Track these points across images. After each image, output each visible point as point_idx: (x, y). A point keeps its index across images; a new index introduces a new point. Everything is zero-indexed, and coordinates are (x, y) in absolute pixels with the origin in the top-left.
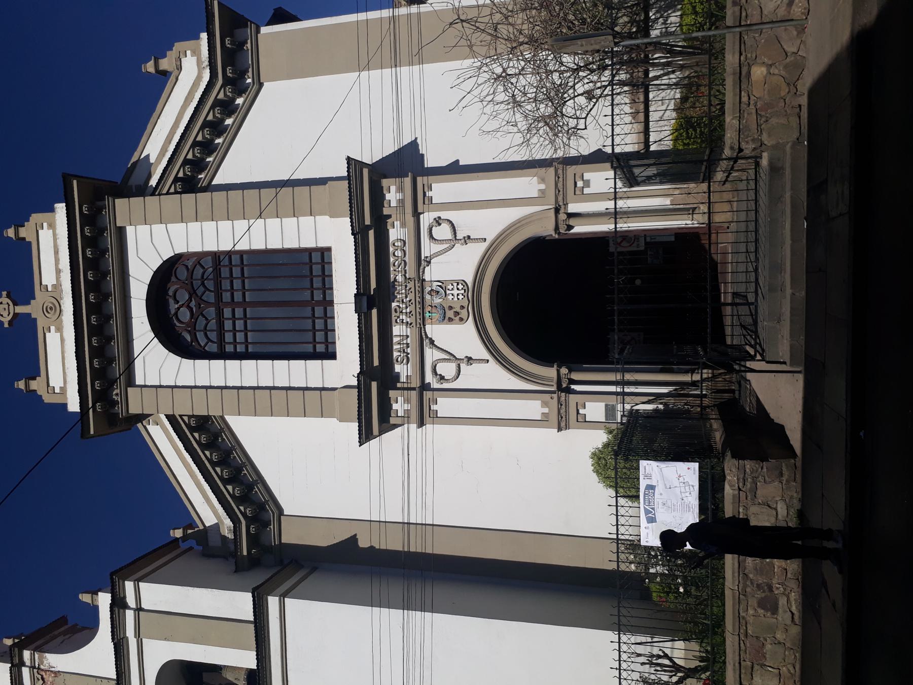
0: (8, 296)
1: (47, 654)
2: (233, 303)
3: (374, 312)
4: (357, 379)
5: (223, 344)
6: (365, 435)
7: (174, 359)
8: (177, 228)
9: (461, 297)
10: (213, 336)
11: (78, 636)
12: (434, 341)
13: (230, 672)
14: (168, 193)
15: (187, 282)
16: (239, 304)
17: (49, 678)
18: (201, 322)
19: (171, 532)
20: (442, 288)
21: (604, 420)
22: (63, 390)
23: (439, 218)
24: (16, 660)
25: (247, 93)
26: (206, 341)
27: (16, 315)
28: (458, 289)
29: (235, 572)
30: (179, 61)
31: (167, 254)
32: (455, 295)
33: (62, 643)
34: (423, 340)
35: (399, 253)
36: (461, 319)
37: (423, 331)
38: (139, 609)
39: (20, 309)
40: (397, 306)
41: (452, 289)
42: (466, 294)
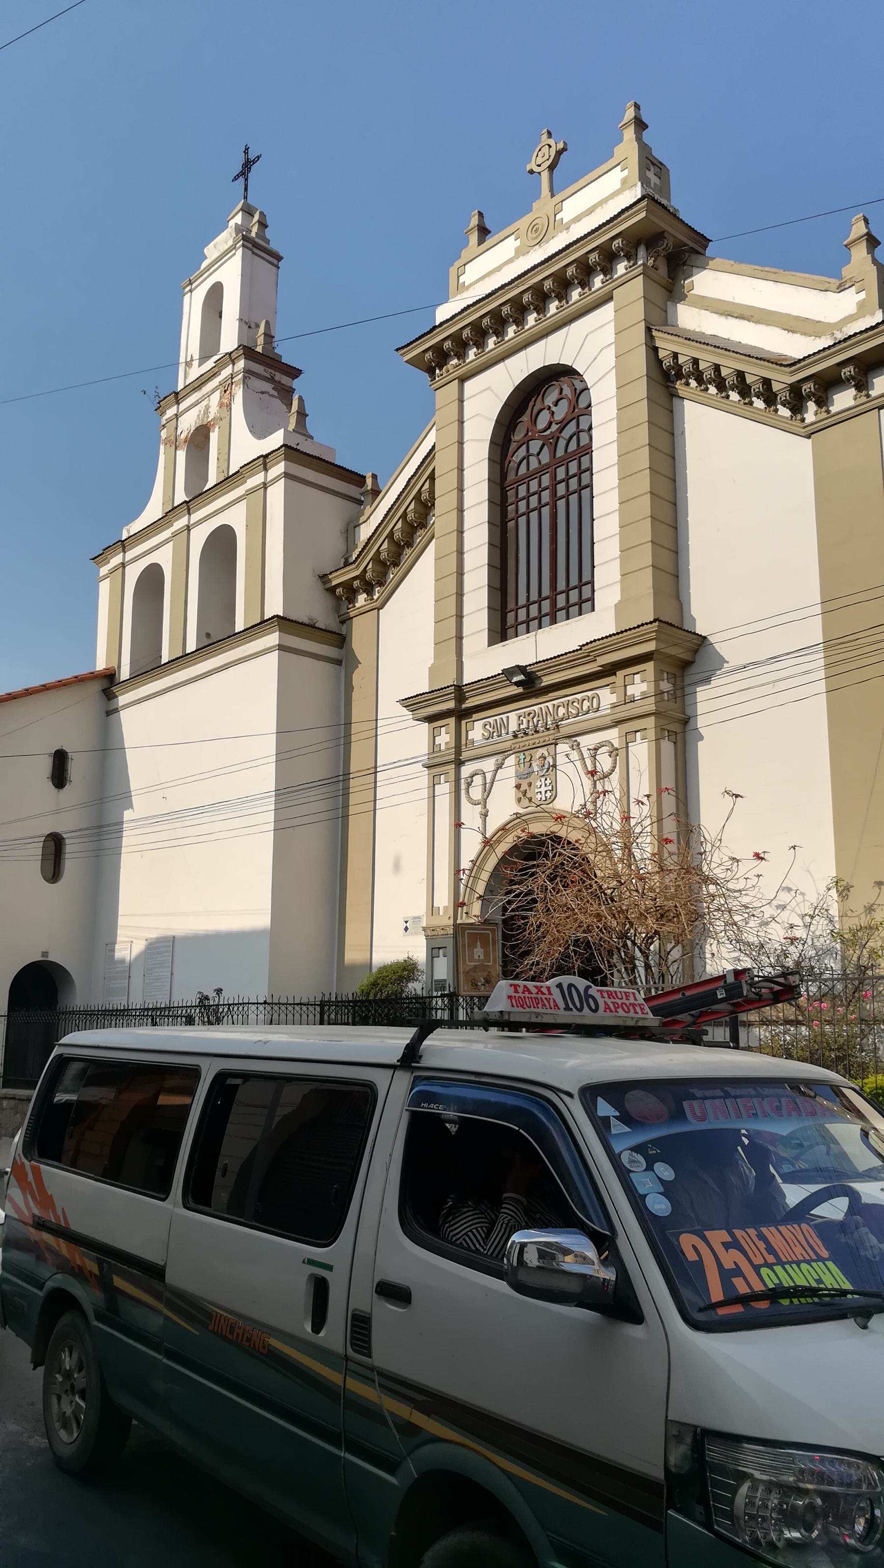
0: (559, 153)
2: (555, 483)
6: (411, 703)
9: (539, 796)
12: (501, 767)
14: (653, 349)
15: (576, 410)
16: (554, 492)
18: (535, 446)
20: (547, 771)
21: (435, 978)
22: (461, 288)
23: (617, 755)
25: (790, 422)
30: (852, 283)
32: (540, 790)
35: (586, 704)
36: (519, 800)
37: (509, 753)
38: (265, 486)
41: (546, 785)
42: (542, 802)
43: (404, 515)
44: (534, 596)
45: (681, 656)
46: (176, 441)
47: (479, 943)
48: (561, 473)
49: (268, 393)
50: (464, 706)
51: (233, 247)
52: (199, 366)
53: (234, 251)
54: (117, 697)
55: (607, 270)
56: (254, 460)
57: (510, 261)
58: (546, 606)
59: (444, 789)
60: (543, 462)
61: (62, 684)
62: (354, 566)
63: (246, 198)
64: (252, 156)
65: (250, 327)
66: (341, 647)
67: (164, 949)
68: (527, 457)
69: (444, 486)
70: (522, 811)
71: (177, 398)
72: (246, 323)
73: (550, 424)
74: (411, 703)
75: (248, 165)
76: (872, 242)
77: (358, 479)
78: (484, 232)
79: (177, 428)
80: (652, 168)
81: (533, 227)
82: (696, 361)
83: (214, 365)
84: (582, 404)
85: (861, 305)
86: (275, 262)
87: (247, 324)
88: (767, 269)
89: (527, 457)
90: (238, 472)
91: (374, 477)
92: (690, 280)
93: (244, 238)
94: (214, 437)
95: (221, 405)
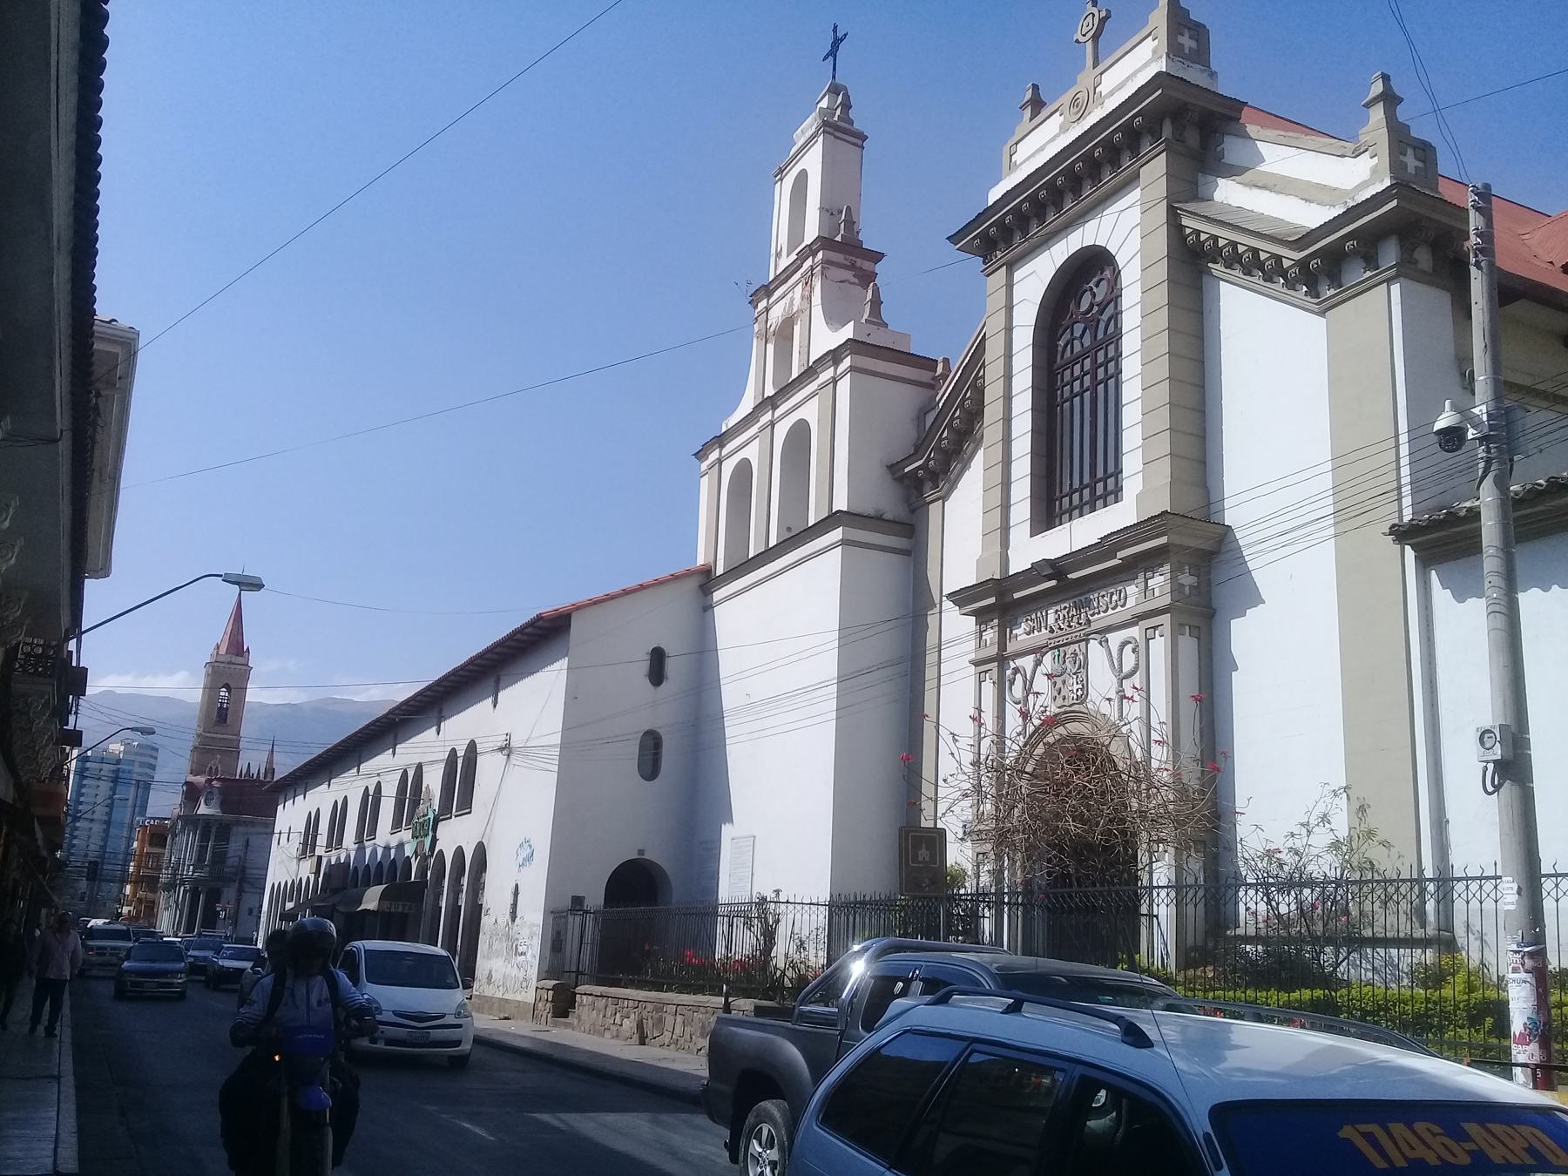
0: (1103, 21)
2: (1096, 366)
3: (1053, 583)
8: (1137, 264)
18: (1078, 328)
22: (1012, 167)
25: (1309, 299)
28: (1077, 690)
29: (887, 466)
31: (1121, 260)
32: (1073, 685)
33: (842, 282)
34: (1039, 651)
35: (1115, 598)
38: (835, 381)
40: (1068, 613)
41: (1077, 683)
42: (1075, 701)
44: (1076, 485)
45: (1202, 547)
47: (924, 846)
48: (1101, 358)
49: (848, 281)
51: (814, 136)
55: (1134, 149)
56: (824, 355)
57: (1053, 139)
58: (1086, 492)
59: (989, 689)
60: (1086, 345)
61: (659, 583)
63: (834, 77)
64: (840, 35)
65: (832, 214)
66: (911, 538)
67: (746, 849)
68: (1070, 342)
69: (993, 372)
70: (1058, 710)
71: (767, 290)
72: (827, 210)
73: (1092, 306)
74: (962, 598)
75: (837, 43)
76: (1390, 99)
77: (929, 364)
78: (1037, 104)
80: (1186, 31)
81: (1074, 102)
82: (1215, 238)
84: (1118, 287)
85: (1374, 171)
86: (859, 142)
87: (827, 211)
88: (1290, 134)
89: (1070, 342)
91: (946, 361)
92: (1222, 146)
93: (825, 124)
94: (797, 329)
95: (803, 297)
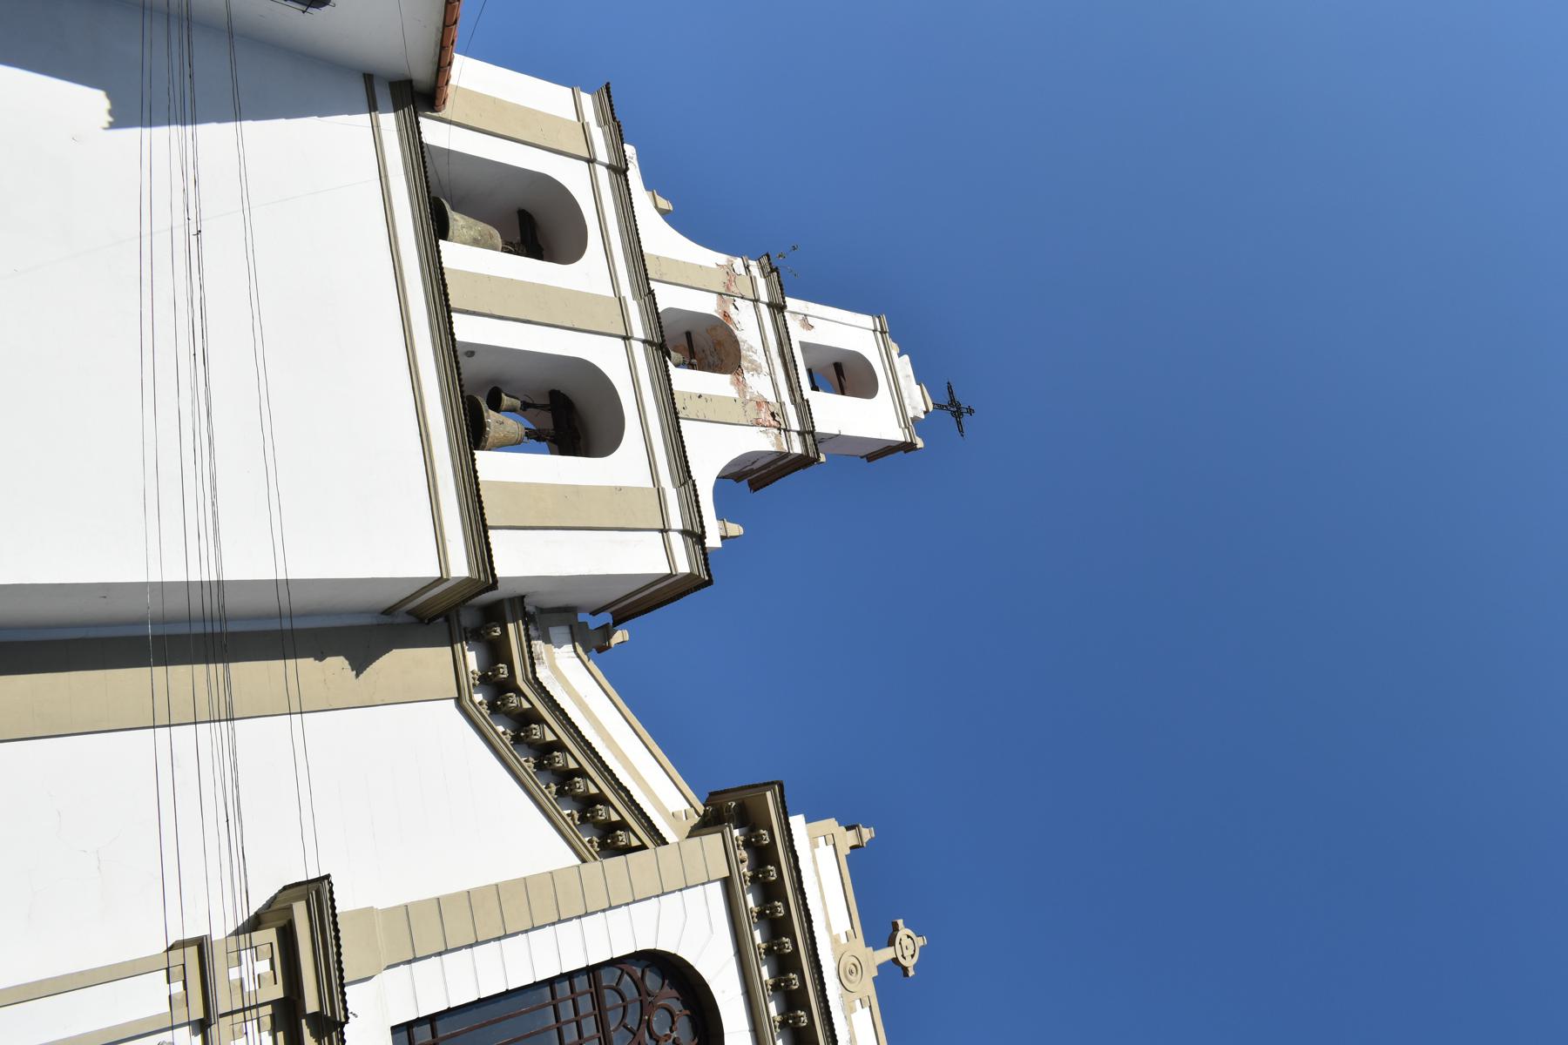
0: (905, 969)
1: (773, 449)
4: (349, 1011)
5: (593, 990)
6: (317, 891)
7: (664, 946)
10: (611, 999)
11: (736, 469)
13: (513, 433)
17: (765, 416)
19: (627, 638)
22: (814, 845)
24: (809, 439)
26: (621, 987)
27: (891, 942)
29: (523, 597)
38: (664, 531)
39: (887, 954)
43: (581, 772)
46: (727, 295)
50: (304, 1021)
52: (800, 342)
53: (903, 426)
54: (395, 110)
56: (701, 517)
62: (530, 676)
66: (409, 613)
71: (777, 308)
79: (742, 298)
83: (805, 398)
90: (690, 477)
95: (761, 403)
